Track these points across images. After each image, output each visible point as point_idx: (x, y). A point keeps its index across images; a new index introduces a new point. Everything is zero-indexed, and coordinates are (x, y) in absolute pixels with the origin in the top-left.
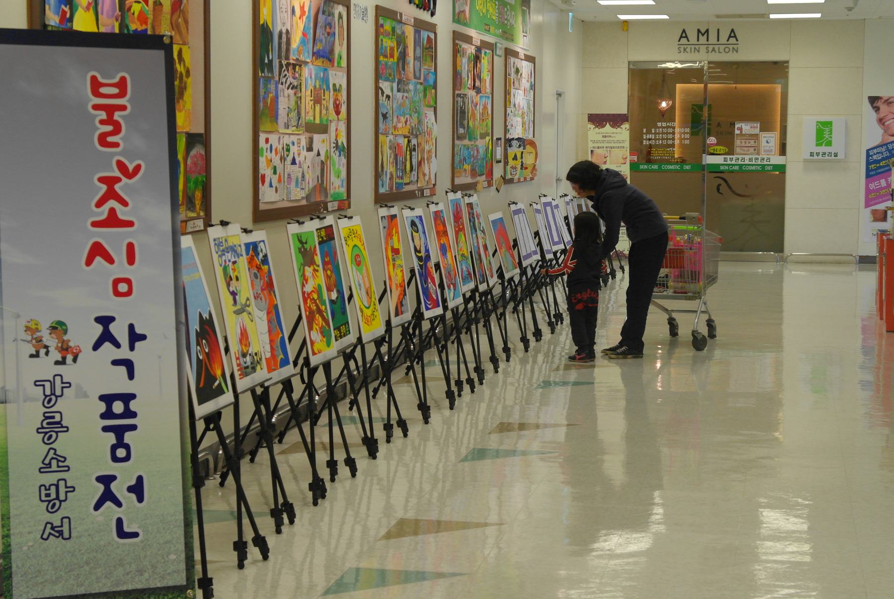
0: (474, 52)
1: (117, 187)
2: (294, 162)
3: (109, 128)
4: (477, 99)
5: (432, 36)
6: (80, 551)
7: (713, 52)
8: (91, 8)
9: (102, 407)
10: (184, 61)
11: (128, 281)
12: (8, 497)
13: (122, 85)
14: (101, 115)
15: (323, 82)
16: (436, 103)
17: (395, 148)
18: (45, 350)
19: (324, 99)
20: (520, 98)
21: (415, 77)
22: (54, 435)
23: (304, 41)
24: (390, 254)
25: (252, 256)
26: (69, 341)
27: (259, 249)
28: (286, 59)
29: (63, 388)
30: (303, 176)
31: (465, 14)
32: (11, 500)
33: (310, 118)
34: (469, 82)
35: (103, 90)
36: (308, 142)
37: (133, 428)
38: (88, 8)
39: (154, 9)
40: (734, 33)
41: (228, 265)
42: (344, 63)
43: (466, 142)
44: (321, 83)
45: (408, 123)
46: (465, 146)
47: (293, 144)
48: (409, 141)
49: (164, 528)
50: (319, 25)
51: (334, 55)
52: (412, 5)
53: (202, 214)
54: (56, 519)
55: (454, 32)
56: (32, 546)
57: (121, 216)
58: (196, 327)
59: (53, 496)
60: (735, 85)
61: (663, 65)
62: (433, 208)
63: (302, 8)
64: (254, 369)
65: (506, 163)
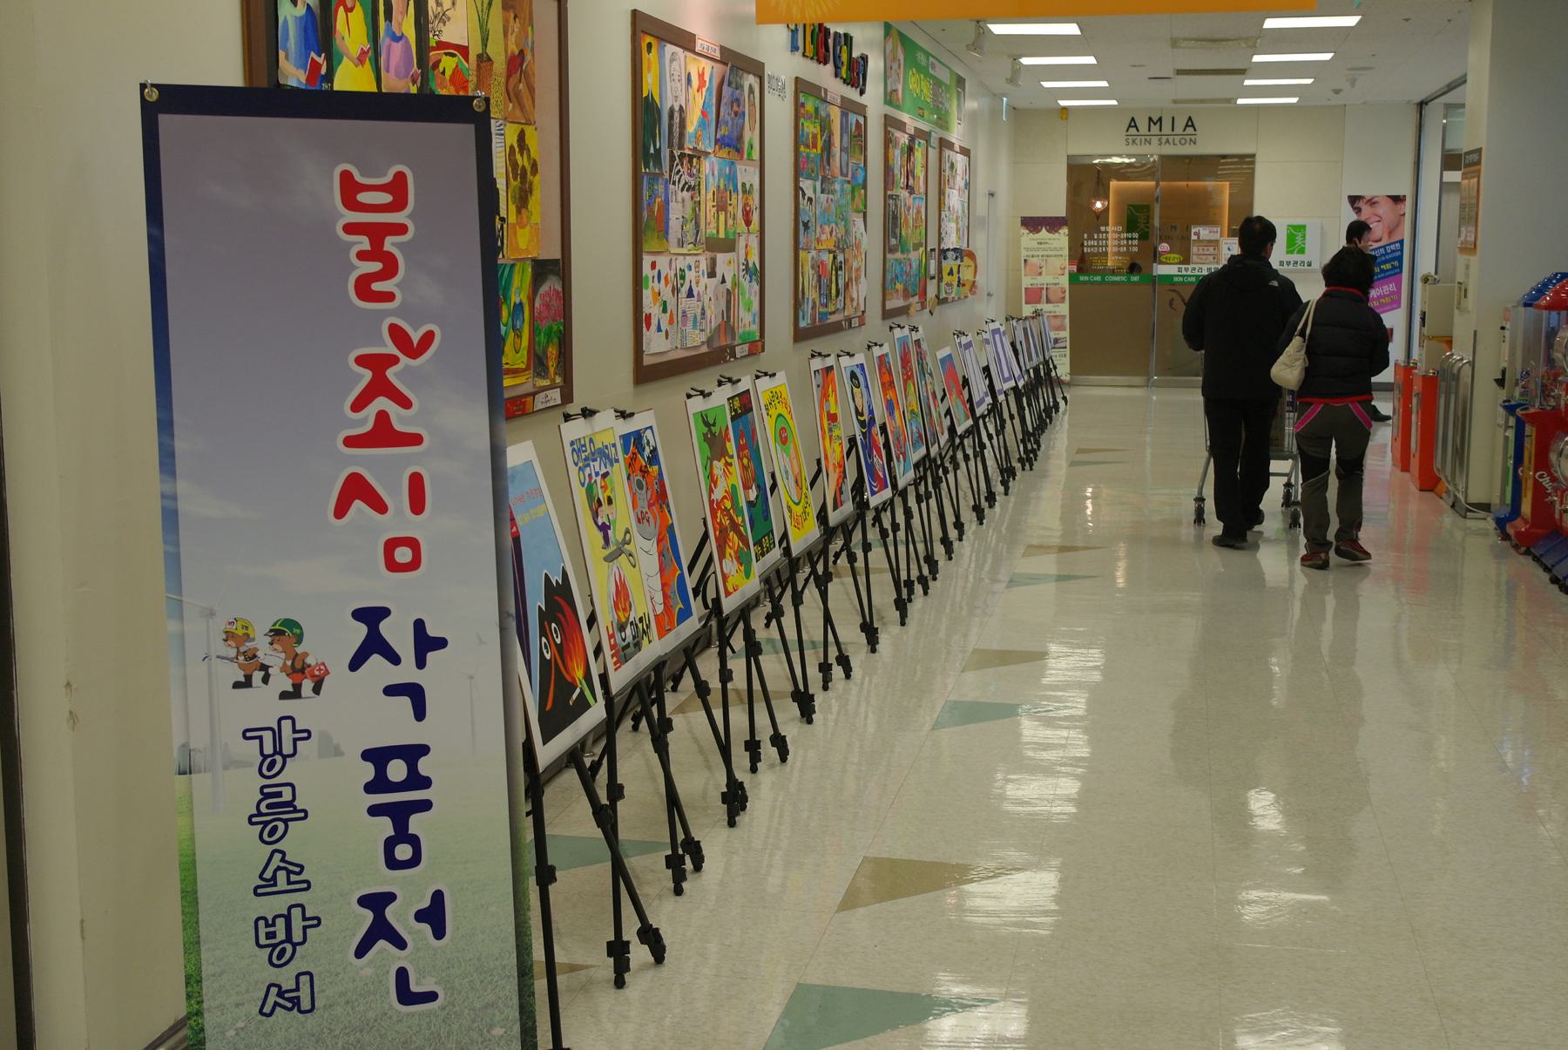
0: (907, 142)
1: (391, 373)
2: (690, 294)
3: (376, 266)
4: (910, 201)
5: (861, 120)
7: (1167, 144)
9: (368, 771)
10: (529, 150)
11: (413, 544)
12: (198, 943)
13: (397, 187)
14: (361, 243)
15: (729, 180)
16: (865, 207)
17: (818, 266)
18: (263, 673)
19: (731, 205)
20: (955, 199)
21: (842, 174)
22: (281, 826)
23: (704, 125)
25: (634, 454)
26: (306, 654)
27: (645, 441)
28: (679, 149)
29: (295, 740)
30: (703, 313)
31: (897, 95)
32: (203, 948)
34: (902, 180)
35: (364, 197)
36: (709, 264)
37: (425, 805)
38: (360, 60)
39: (478, 65)
40: (1192, 122)
41: (595, 481)
42: (756, 155)
43: (898, 255)
44: (726, 182)
45: (834, 233)
46: (896, 260)
47: (690, 268)
48: (835, 258)
49: (482, 982)
50: (724, 101)
51: (743, 143)
52: (838, 79)
53: (558, 380)
54: (286, 977)
55: (886, 116)
56: (242, 1029)
57: (398, 426)
58: (539, 604)
59: (281, 936)
60: (1186, 183)
61: (1108, 160)
62: (877, 351)
63: (701, 76)
64: (638, 646)
65: (940, 279)
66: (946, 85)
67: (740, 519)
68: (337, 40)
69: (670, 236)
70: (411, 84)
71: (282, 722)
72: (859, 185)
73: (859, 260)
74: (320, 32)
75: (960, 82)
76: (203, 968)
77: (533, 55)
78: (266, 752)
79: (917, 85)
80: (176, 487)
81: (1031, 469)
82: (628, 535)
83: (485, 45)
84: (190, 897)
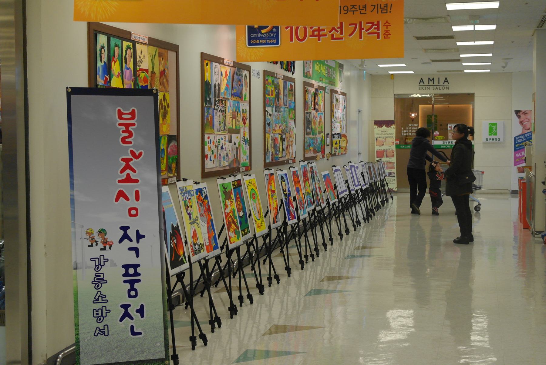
0: (314, 91)
1: (131, 163)
2: (222, 148)
3: (127, 135)
4: (316, 115)
5: (293, 84)
6: (113, 341)
8: (120, 76)
9: (123, 271)
12: (78, 315)
13: (133, 113)
15: (237, 108)
16: (295, 117)
17: (274, 140)
18: (96, 243)
19: (238, 117)
20: (339, 113)
21: (284, 105)
22: (100, 285)
24: (270, 193)
25: (199, 195)
26: (107, 238)
27: (203, 192)
28: (218, 98)
29: (104, 261)
30: (227, 155)
31: (310, 73)
33: (230, 126)
34: (312, 106)
35: (124, 116)
37: (139, 281)
38: (118, 76)
39: (151, 75)
41: (187, 200)
42: (248, 99)
43: (311, 136)
44: (236, 109)
47: (222, 139)
48: (281, 136)
49: (154, 330)
50: (235, 80)
51: (242, 95)
52: (282, 69)
53: (176, 174)
54: (101, 326)
55: (304, 82)
56: (89, 339)
57: (132, 177)
58: (170, 231)
59: (100, 314)
63: (226, 72)
64: (200, 251)
65: (332, 146)
66: (333, 68)
67: (236, 220)
68: (112, 71)
69: (215, 128)
70: (132, 82)
71: (101, 256)
72: (292, 109)
73: (292, 137)
74: (108, 69)
75: (341, 66)
76: (79, 322)
77: (168, 70)
78: (96, 264)
79: (320, 69)
80: (74, 193)
81: (368, 222)
82: (197, 218)
83: (153, 67)
84: (76, 302)
